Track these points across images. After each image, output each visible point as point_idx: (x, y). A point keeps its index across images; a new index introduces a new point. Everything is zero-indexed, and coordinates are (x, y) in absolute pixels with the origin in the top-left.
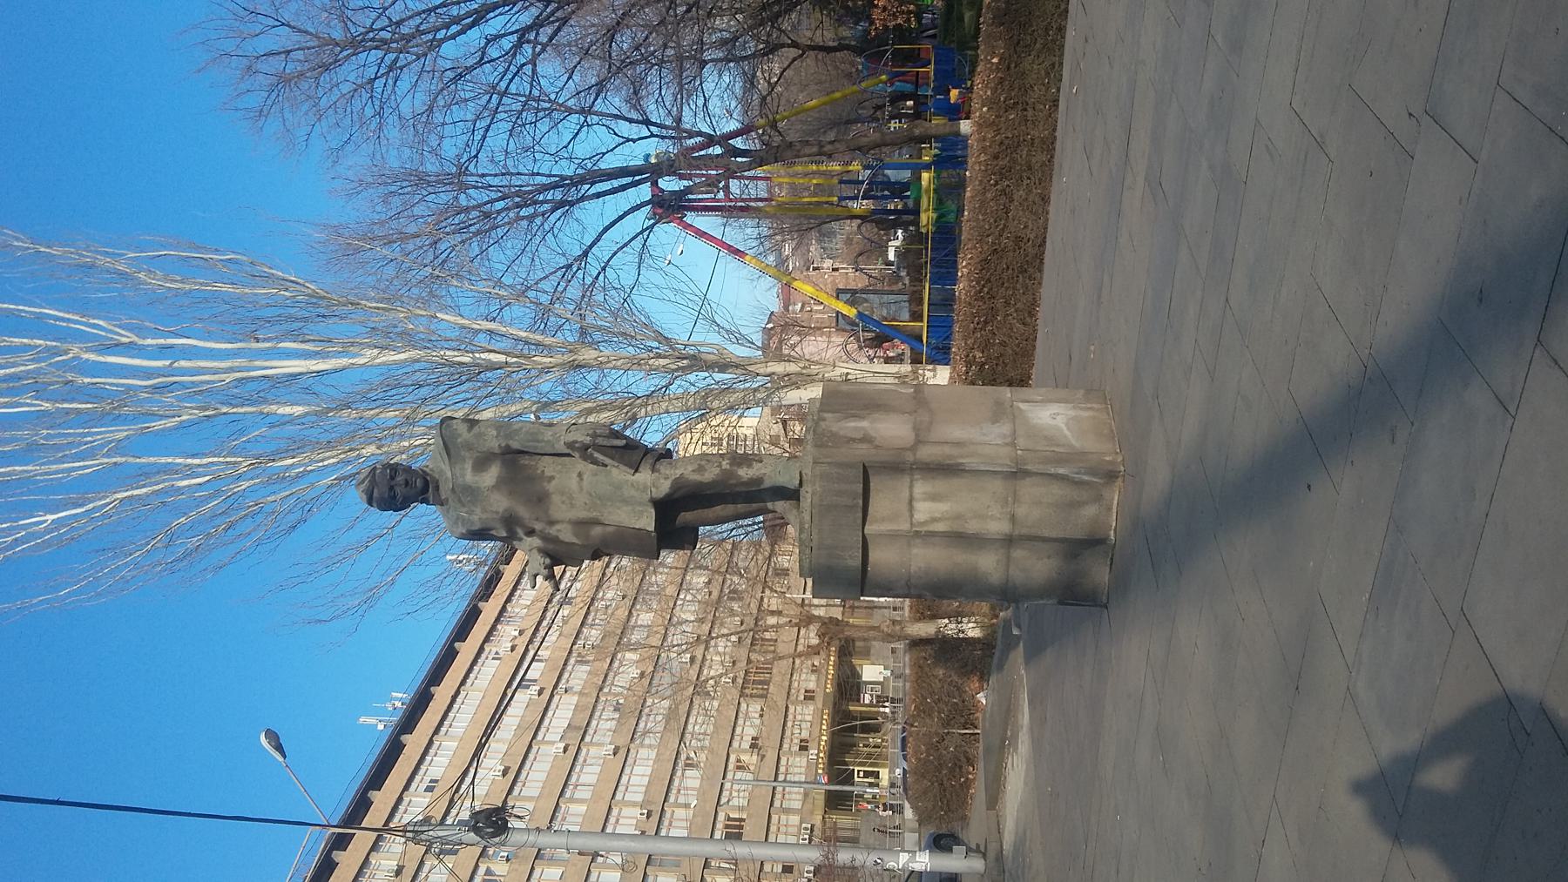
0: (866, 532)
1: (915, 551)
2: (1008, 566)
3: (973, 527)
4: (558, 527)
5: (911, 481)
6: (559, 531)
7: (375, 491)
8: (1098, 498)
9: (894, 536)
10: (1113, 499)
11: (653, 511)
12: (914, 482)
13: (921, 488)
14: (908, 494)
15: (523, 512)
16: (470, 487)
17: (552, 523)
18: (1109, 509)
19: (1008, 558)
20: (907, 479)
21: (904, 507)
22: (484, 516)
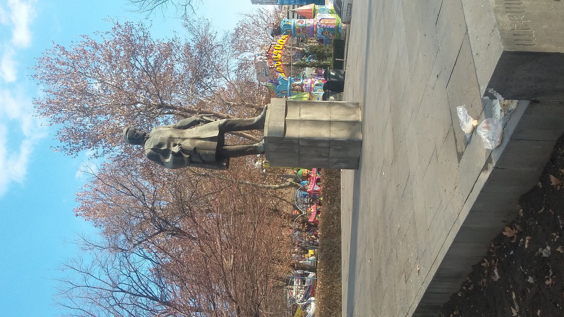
0: (286, 119)
1: (301, 129)
2: (330, 132)
3: (318, 118)
4: (186, 141)
5: (300, 108)
6: (185, 142)
7: (130, 128)
8: (355, 113)
9: (294, 121)
10: (359, 113)
11: (218, 132)
12: (301, 109)
13: (303, 111)
14: (299, 113)
15: (176, 136)
16: (161, 131)
17: (184, 139)
18: (359, 116)
19: (330, 131)
20: (298, 108)
21: (298, 116)
22: (162, 137)
